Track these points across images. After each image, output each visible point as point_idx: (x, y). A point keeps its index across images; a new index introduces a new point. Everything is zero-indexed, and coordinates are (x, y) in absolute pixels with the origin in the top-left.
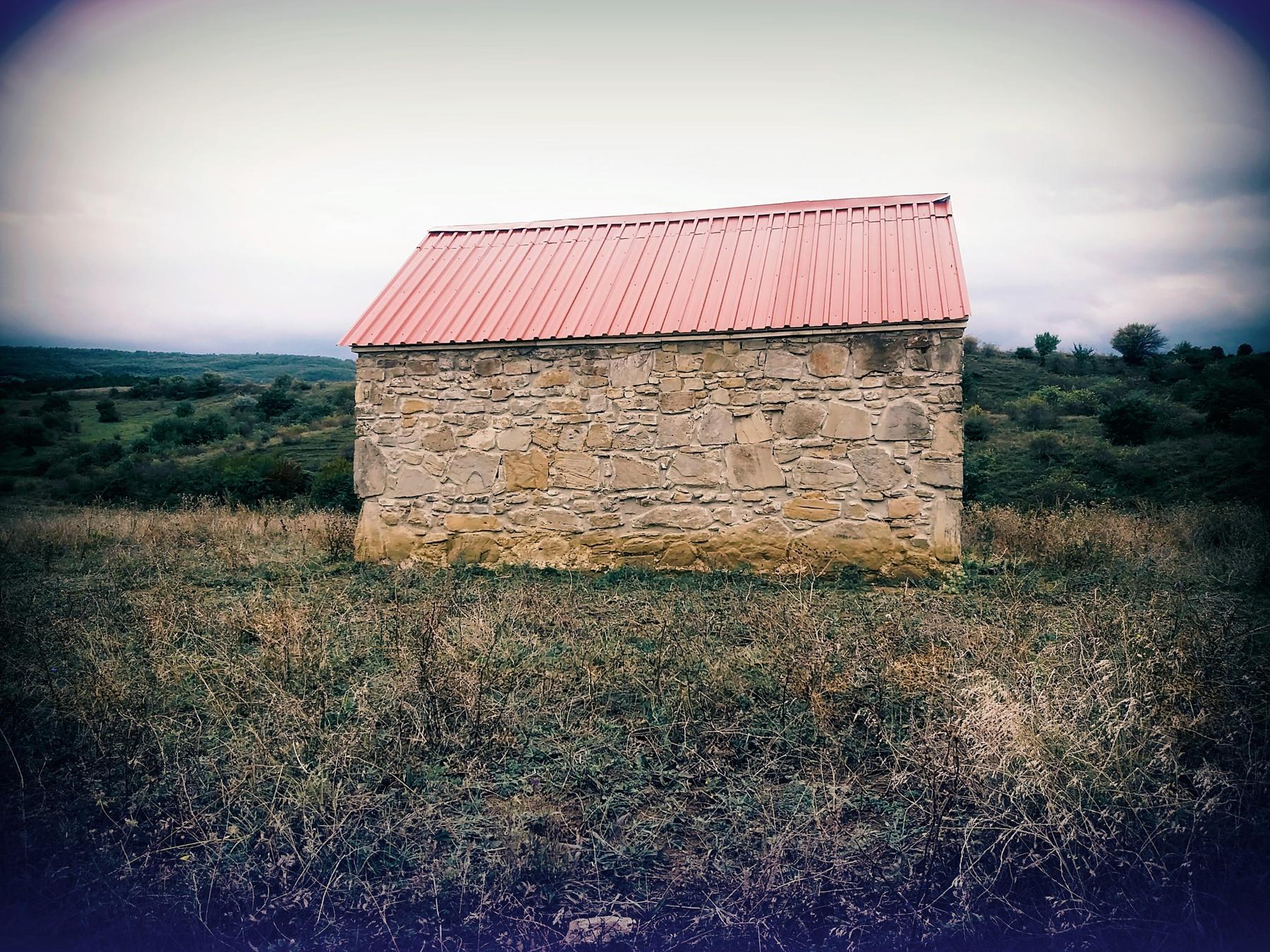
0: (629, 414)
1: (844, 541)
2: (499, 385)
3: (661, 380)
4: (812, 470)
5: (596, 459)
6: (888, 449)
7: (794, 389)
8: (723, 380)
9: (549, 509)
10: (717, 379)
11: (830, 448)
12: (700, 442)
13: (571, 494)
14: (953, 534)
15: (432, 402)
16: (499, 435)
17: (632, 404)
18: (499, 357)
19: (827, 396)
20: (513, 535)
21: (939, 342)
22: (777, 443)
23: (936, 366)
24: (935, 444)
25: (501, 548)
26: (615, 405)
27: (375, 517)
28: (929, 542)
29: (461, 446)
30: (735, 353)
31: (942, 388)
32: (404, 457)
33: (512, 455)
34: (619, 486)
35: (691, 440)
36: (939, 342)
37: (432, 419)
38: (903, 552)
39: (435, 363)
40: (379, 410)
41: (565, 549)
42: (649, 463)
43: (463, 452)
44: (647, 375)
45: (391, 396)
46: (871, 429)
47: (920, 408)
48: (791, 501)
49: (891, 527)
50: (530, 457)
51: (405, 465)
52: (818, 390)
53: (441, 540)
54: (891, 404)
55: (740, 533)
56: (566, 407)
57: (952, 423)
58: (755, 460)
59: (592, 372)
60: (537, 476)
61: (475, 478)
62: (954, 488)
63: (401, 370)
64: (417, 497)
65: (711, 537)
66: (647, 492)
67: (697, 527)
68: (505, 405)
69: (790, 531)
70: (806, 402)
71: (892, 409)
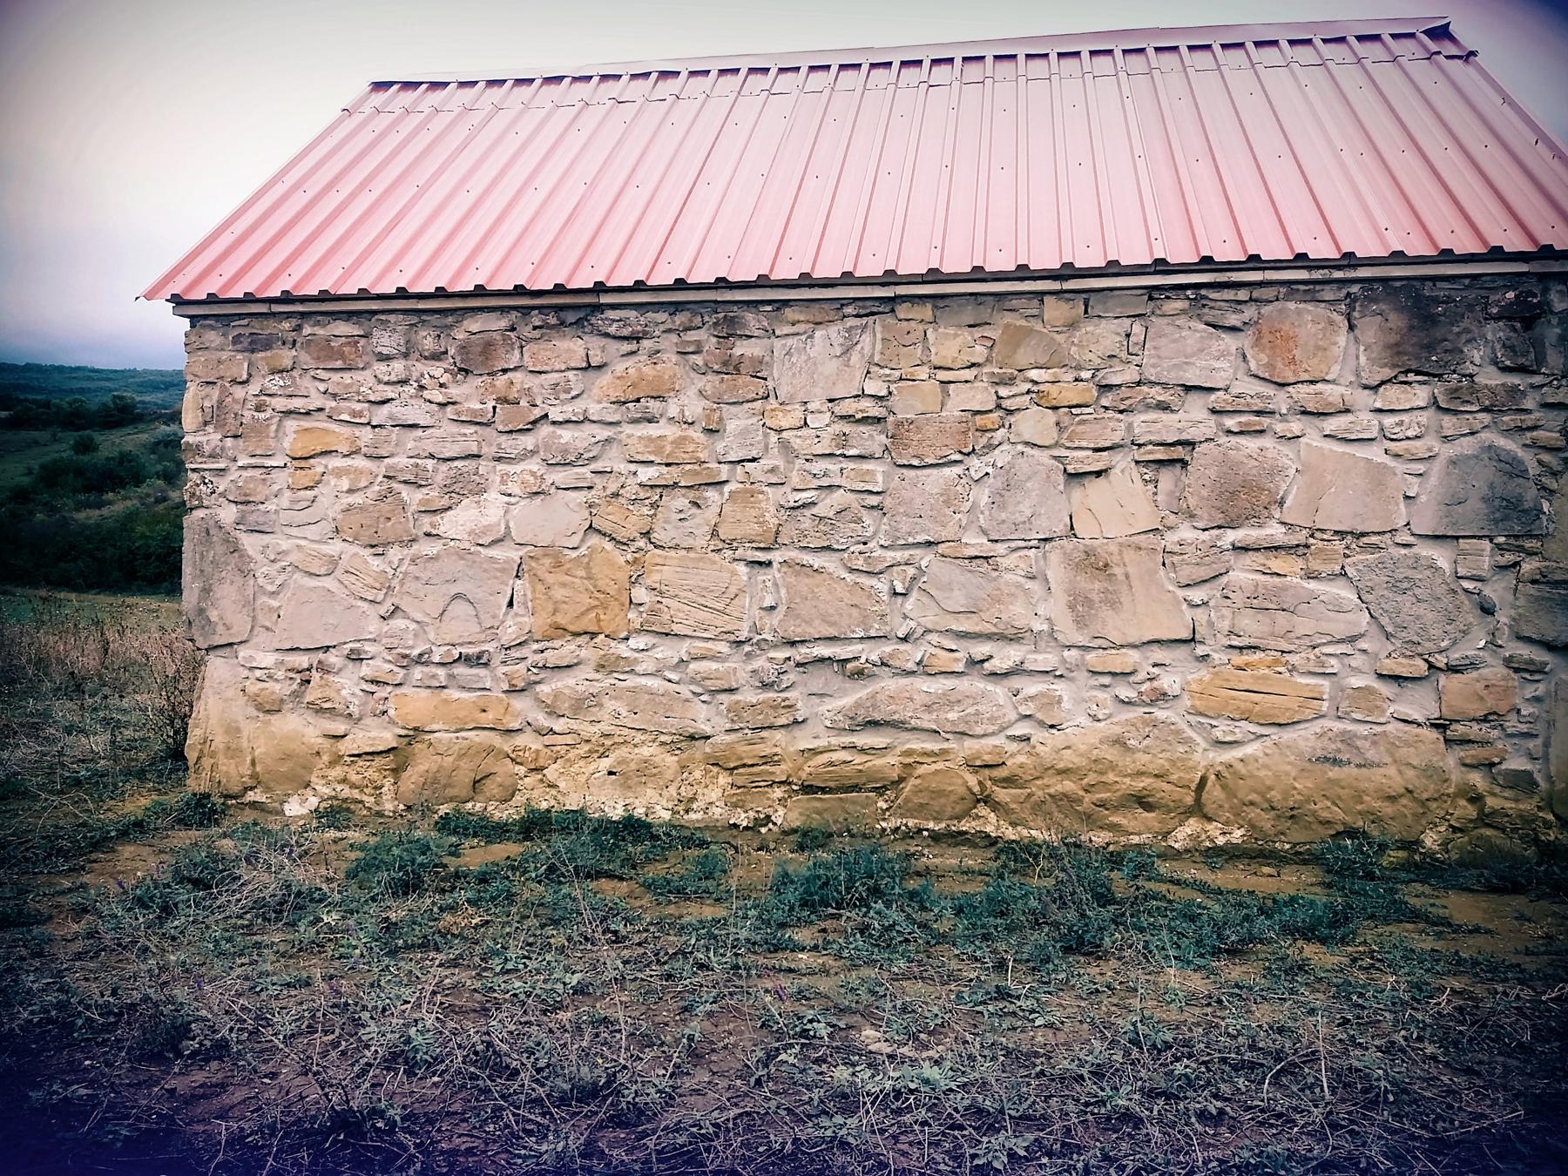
0: (819, 466)
1: (1334, 773)
2: (513, 395)
3: (893, 387)
4: (1259, 603)
5: (742, 569)
7: (1214, 411)
8: (1041, 387)
9: (632, 681)
10: (1028, 386)
11: (1301, 551)
12: (985, 532)
13: (683, 649)
15: (357, 431)
16: (515, 511)
18: (513, 329)
19: (1295, 426)
20: (548, 740)
22: (1171, 539)
25: (522, 770)
26: (785, 446)
27: (230, 693)
28: (1538, 777)
29: (428, 535)
30: (1072, 325)
32: (293, 558)
33: (545, 555)
34: (795, 632)
37: (359, 472)
38: (1476, 799)
39: (362, 342)
41: (669, 775)
43: (428, 548)
44: (859, 374)
45: (262, 415)
46: (1402, 506)
47: (1521, 462)
48: (1204, 673)
49: (1447, 741)
51: (297, 576)
52: (1273, 413)
54: (1449, 451)
55: (1083, 748)
56: (668, 449)
58: (1121, 577)
59: (732, 367)
61: (460, 608)
63: (286, 356)
66: (860, 647)
67: (979, 730)
68: (528, 441)
69: (1203, 745)
70: (1243, 441)
71: (1453, 462)
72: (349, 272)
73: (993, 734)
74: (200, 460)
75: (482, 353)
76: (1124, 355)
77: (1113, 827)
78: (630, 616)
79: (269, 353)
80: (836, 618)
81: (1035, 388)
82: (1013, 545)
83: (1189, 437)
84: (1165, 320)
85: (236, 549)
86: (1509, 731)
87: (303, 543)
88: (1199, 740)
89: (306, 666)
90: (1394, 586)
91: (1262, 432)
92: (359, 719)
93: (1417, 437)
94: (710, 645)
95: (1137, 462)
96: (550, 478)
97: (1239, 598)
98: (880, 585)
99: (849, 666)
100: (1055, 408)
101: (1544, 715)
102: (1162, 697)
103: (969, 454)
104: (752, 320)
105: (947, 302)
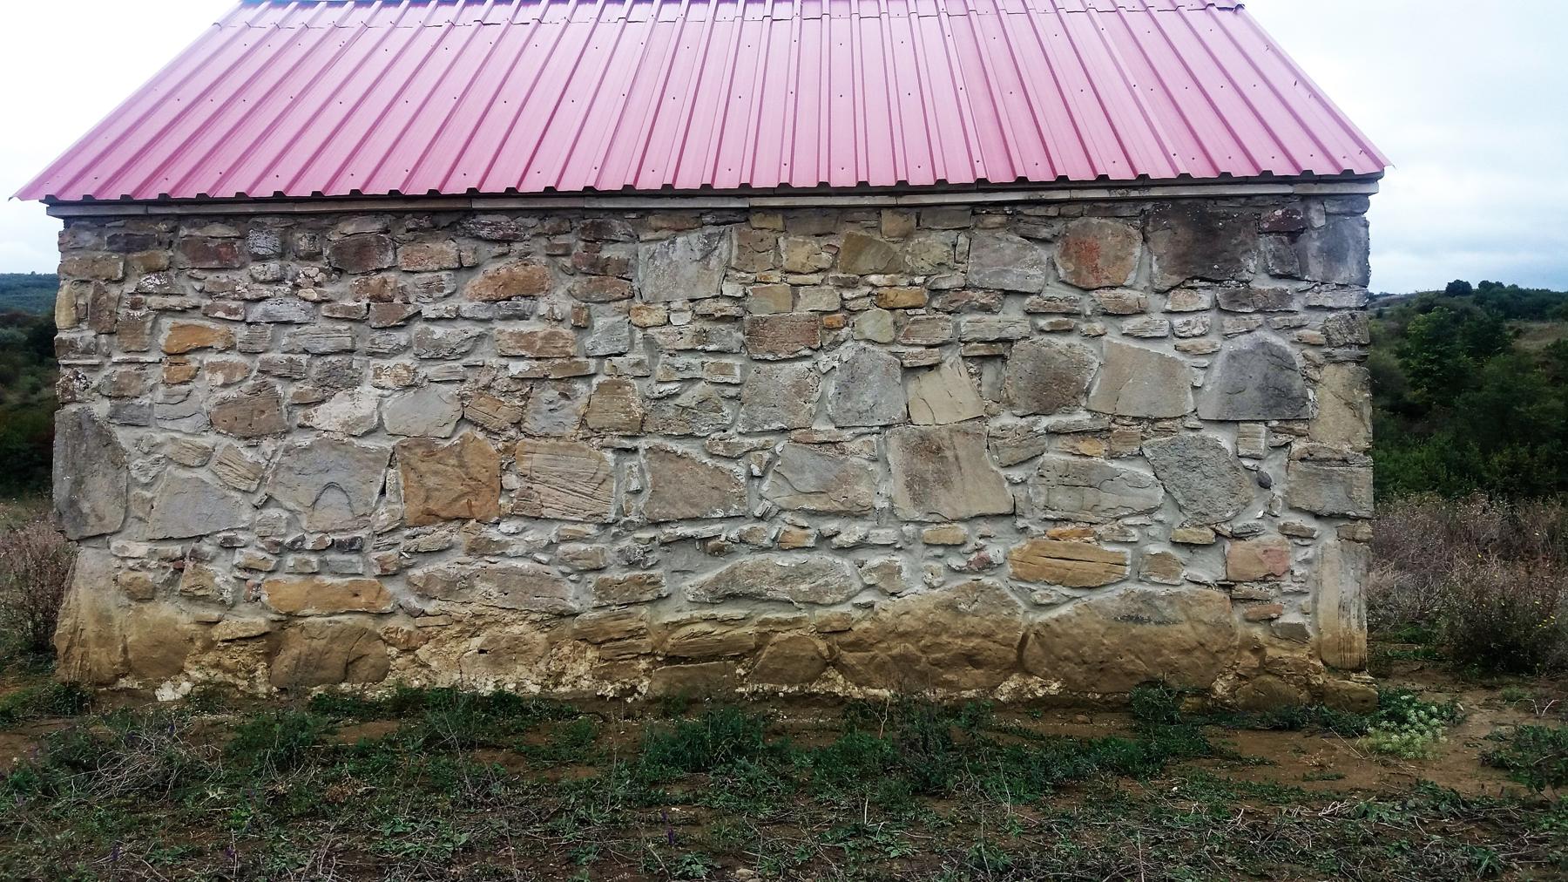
0: (681, 361)
1: (1136, 630)
2: (388, 293)
3: (748, 289)
4: (1073, 480)
5: (609, 456)
6: (1225, 439)
7: (1028, 313)
9: (503, 564)
10: (868, 290)
12: (832, 420)
13: (553, 532)
14: (1354, 612)
15: (232, 328)
16: (388, 403)
17: (688, 338)
18: (386, 231)
19: (1098, 326)
20: (419, 621)
21: (1323, 222)
22: (994, 424)
23: (1316, 269)
24: (1318, 430)
25: (393, 651)
26: (649, 342)
27: (102, 583)
28: (1309, 629)
29: (301, 427)
30: (907, 236)
31: (1331, 316)
32: (167, 450)
34: (659, 512)
35: (815, 417)
36: (1323, 222)
37: (233, 367)
38: (1258, 650)
39: (238, 243)
40: (109, 344)
41: (539, 651)
42: (723, 464)
43: (304, 440)
44: (717, 277)
45: (137, 313)
46: (1190, 396)
47: (1290, 356)
48: (1023, 543)
50: (459, 453)
52: (1078, 314)
53: (254, 633)
54: (1229, 347)
55: (920, 612)
56: (539, 344)
57: (1351, 386)
58: (951, 459)
59: (599, 268)
60: (475, 492)
61: (332, 497)
62: (1356, 519)
63: (163, 257)
64: (200, 538)
65: (858, 621)
66: (720, 526)
67: (828, 600)
68: (401, 337)
69: (1024, 607)
70: (1054, 339)
71: (1233, 357)
72: (225, 177)
73: (841, 602)
74: (73, 356)
75: (356, 253)
76: (951, 263)
77: (948, 684)
78: (501, 501)
79: (145, 254)
80: (697, 500)
81: (875, 292)
82: (858, 431)
83: (1008, 335)
84: (985, 233)
85: (108, 441)
86: (1285, 589)
87: (177, 435)
88: (1020, 603)
89: (179, 554)
90: (1185, 465)
91: (1069, 331)
92: (233, 606)
93: (1202, 335)
94: (578, 527)
95: (964, 358)
96: (423, 372)
97: (1052, 476)
98: (738, 469)
99: (711, 544)
100: (892, 309)
101: (1313, 575)
102: (987, 565)
103: (817, 350)
104: (618, 227)
105: (796, 213)
